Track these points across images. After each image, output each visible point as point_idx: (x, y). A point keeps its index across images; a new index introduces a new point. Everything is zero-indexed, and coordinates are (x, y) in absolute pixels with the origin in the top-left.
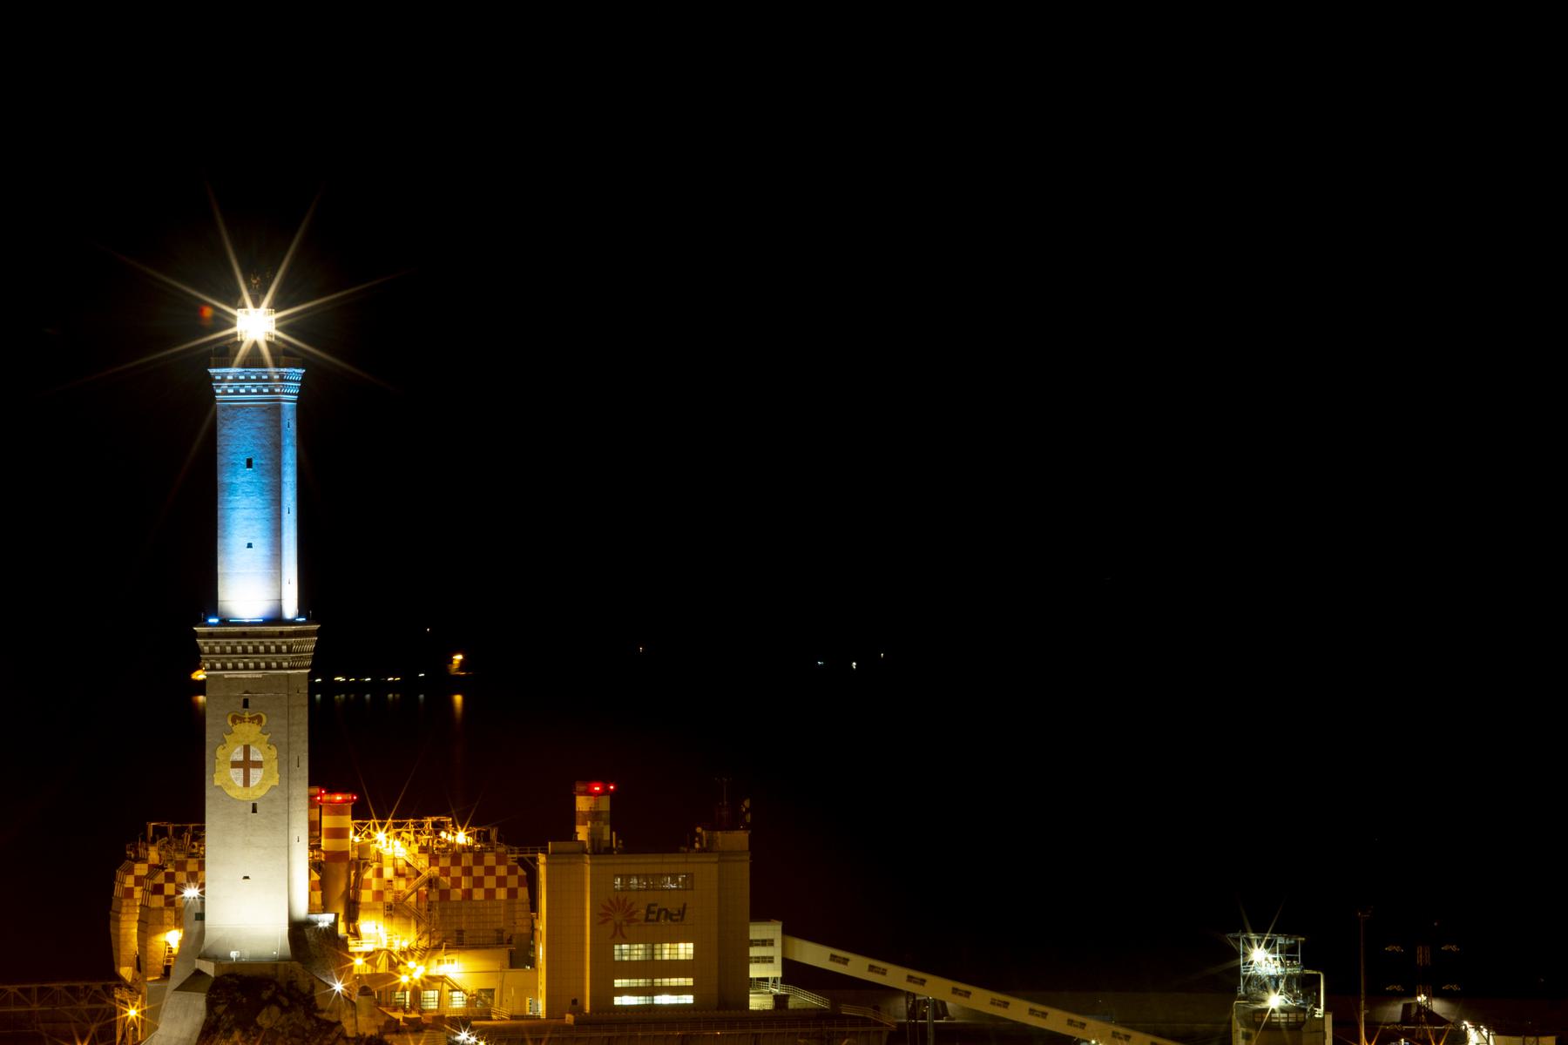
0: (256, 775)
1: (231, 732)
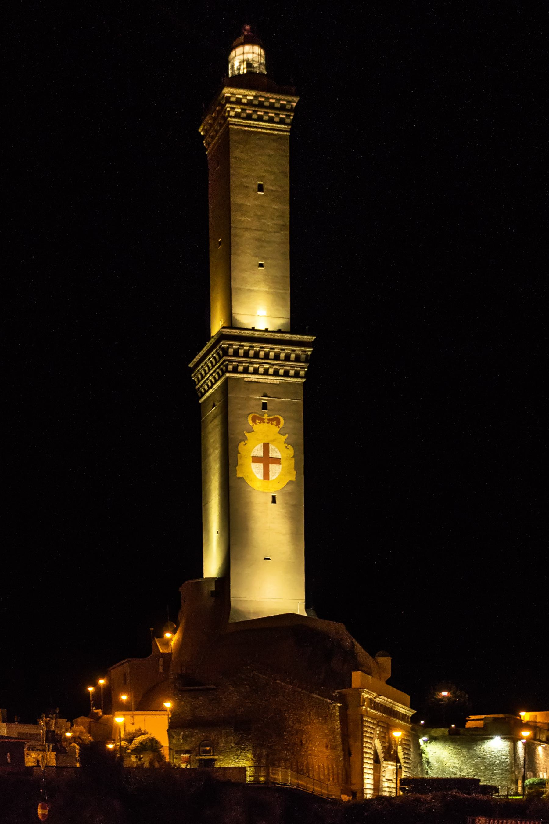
0: (275, 470)
1: (251, 431)
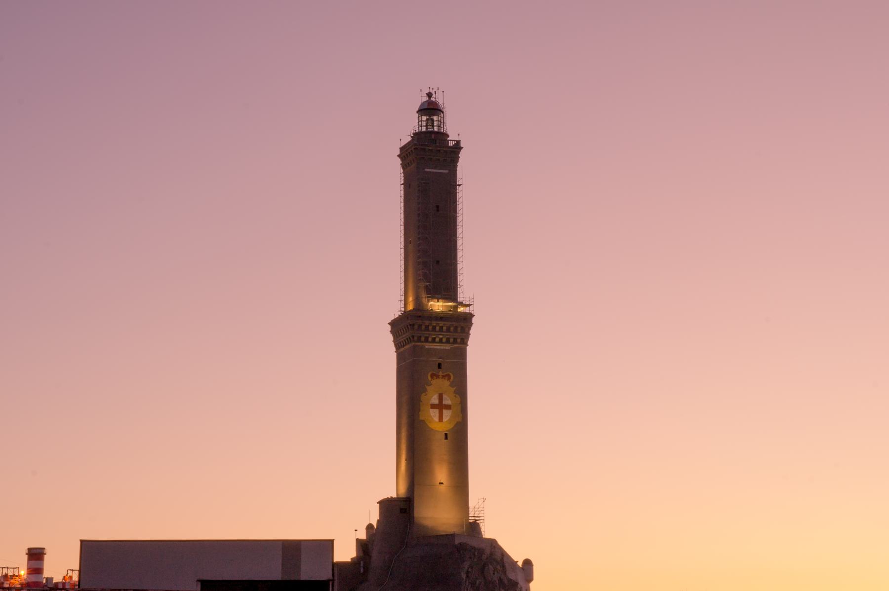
0: (447, 414)
